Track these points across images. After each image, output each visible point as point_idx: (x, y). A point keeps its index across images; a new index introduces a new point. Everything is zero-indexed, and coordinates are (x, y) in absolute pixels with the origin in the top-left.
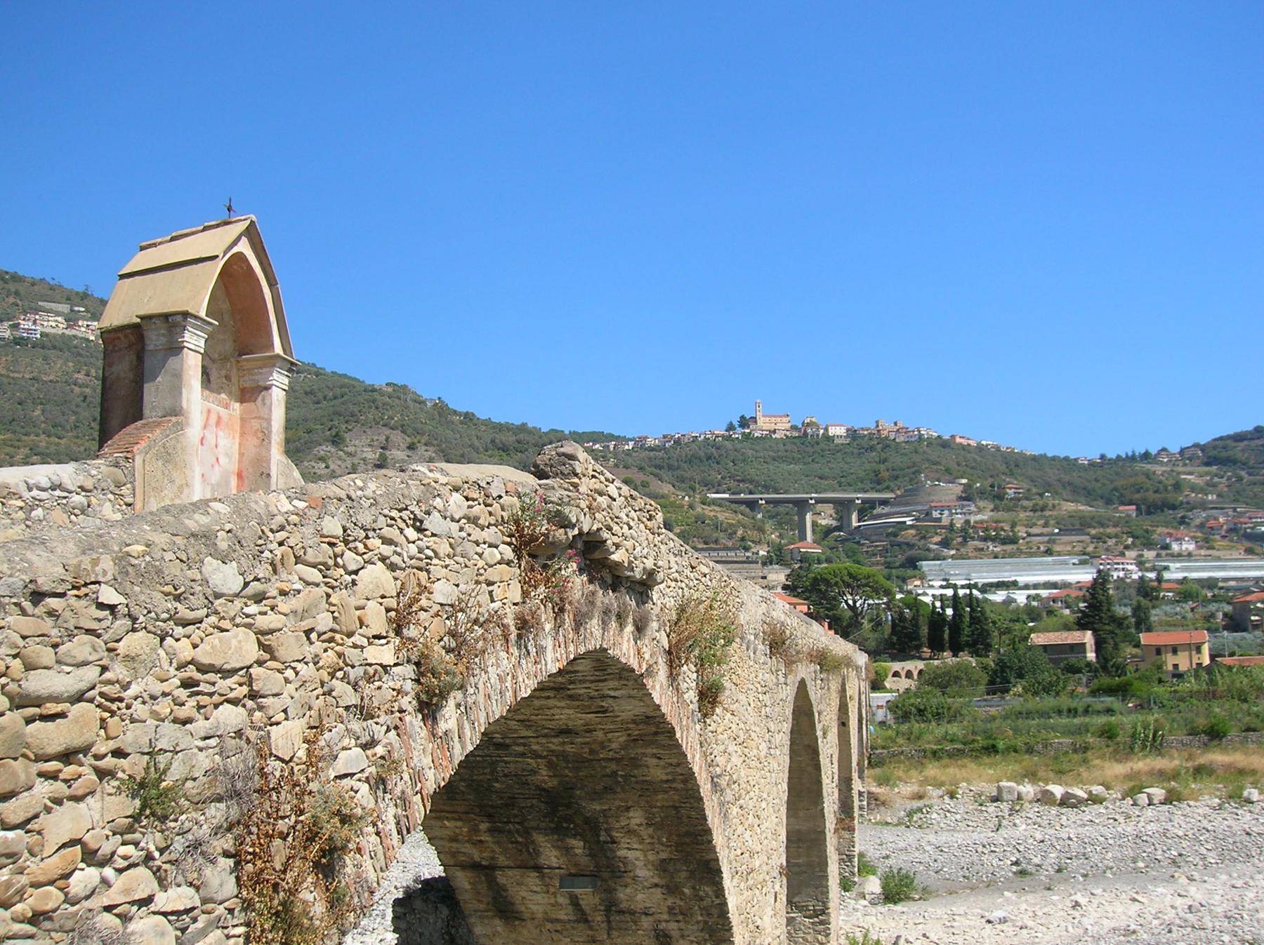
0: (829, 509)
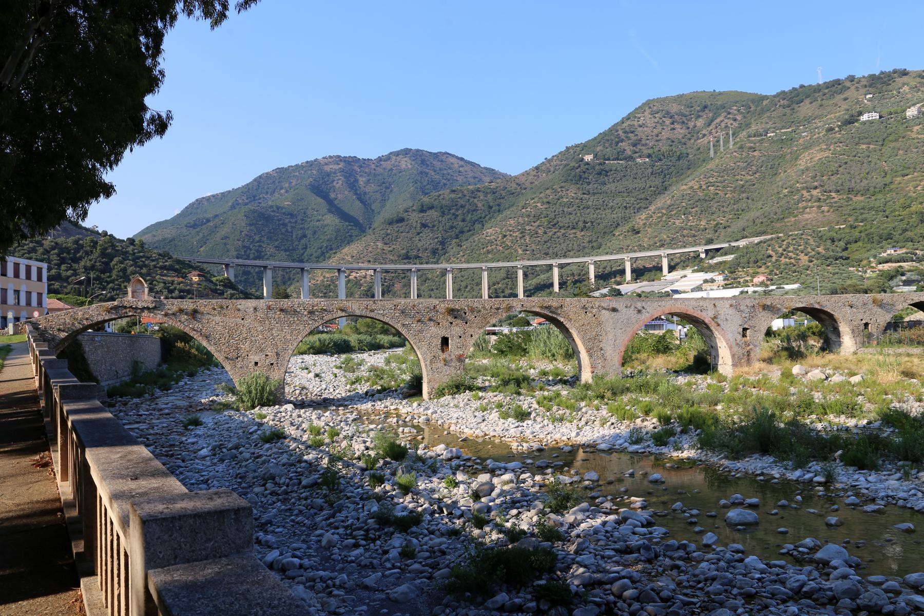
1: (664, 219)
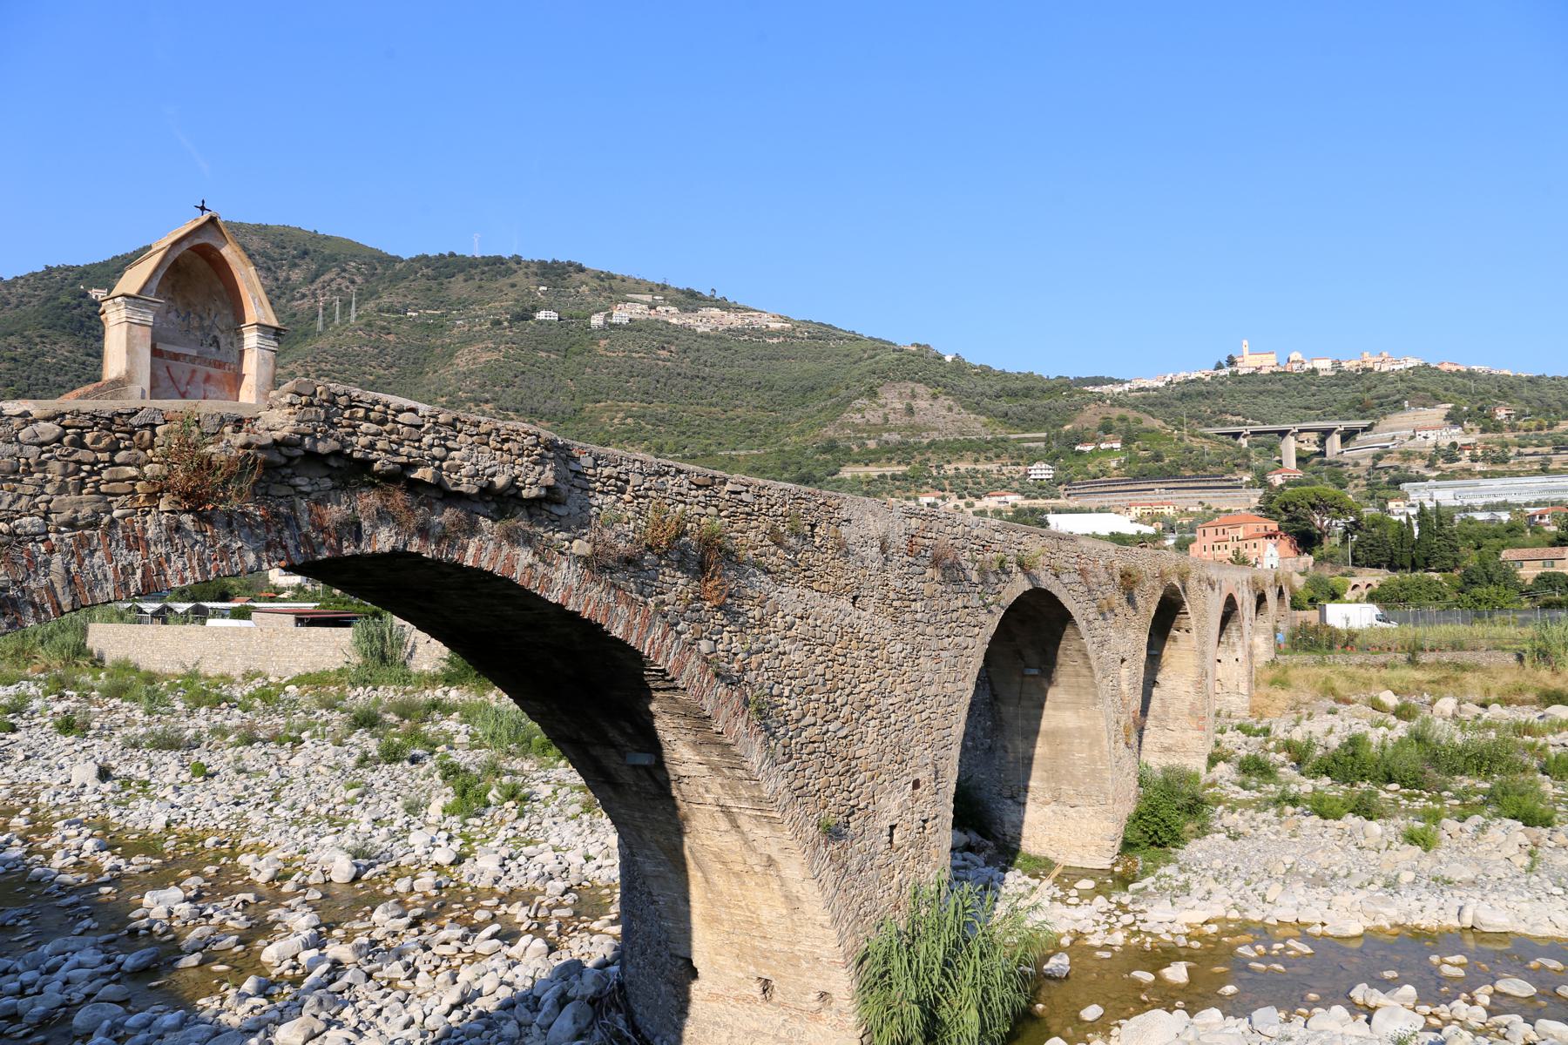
0: (1314, 436)
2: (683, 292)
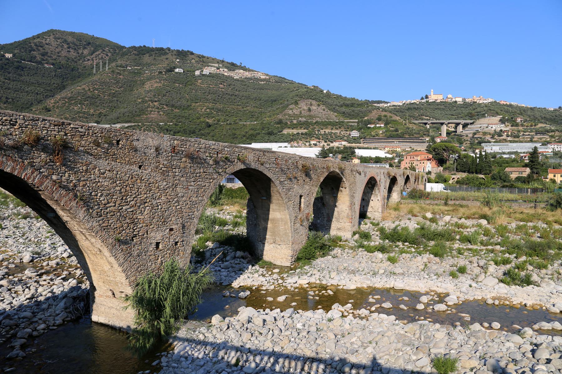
0: (453, 125)
1: (67, 105)
2: (230, 63)
